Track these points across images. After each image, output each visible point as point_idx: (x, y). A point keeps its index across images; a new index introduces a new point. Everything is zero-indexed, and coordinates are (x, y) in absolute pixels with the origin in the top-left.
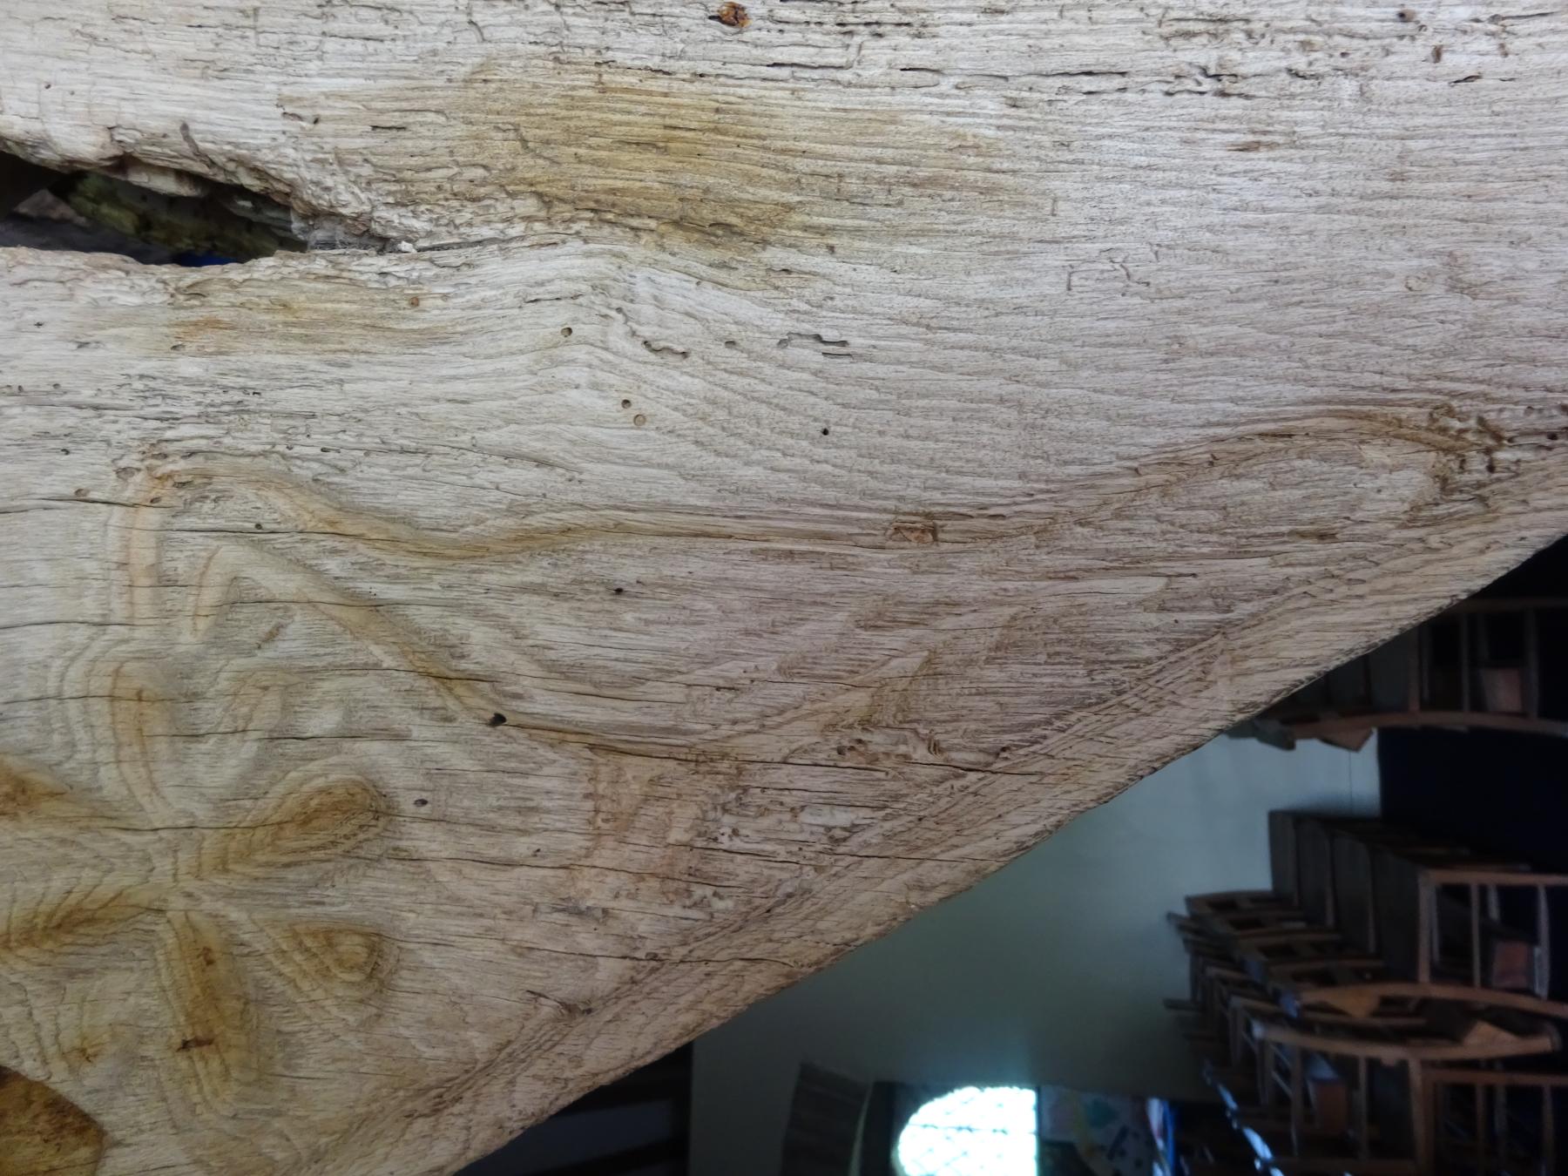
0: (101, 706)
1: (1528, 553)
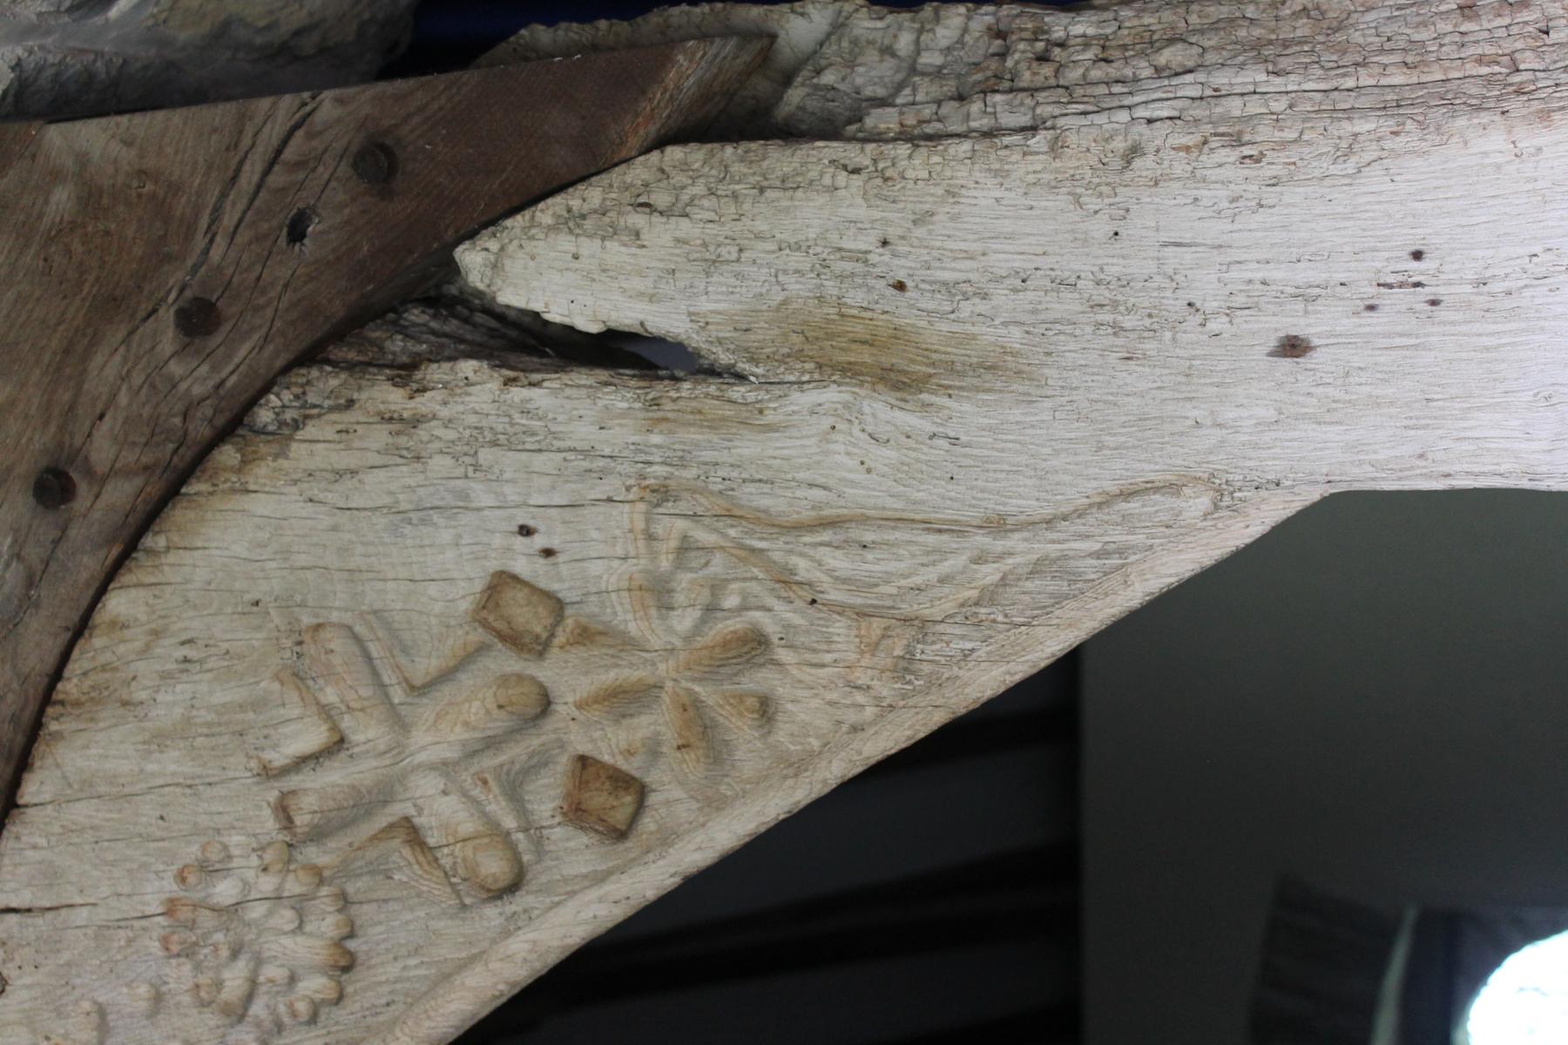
0: (626, 594)
1: (1267, 528)
